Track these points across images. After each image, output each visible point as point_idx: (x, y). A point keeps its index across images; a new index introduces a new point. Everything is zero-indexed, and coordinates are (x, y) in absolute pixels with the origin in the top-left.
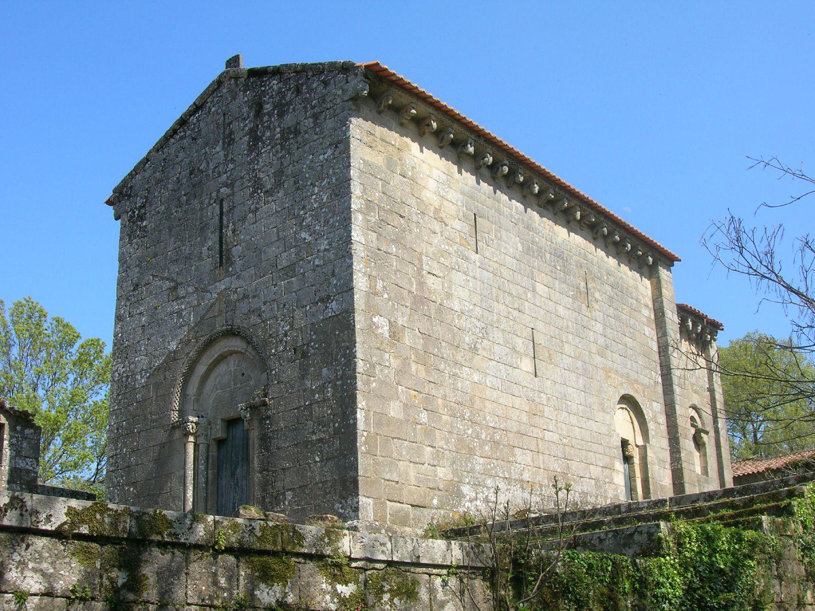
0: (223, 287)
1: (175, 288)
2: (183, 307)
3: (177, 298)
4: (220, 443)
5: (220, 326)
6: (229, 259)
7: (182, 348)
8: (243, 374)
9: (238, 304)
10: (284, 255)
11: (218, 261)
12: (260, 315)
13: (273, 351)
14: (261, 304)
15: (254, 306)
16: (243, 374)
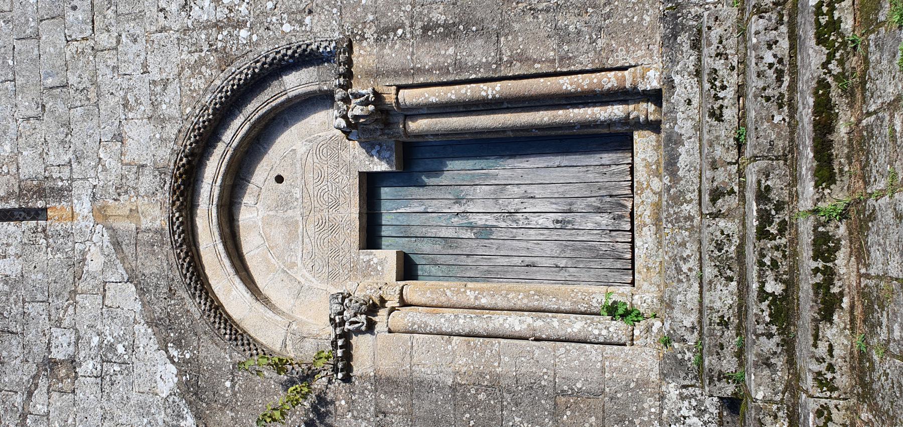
0: (87, 205)
1: (50, 365)
2: (95, 340)
3: (72, 362)
4: (408, 269)
5: (156, 215)
6: (41, 192)
7: (178, 344)
8: (279, 179)
9: (126, 159)
10: (70, 16)
11: (33, 223)
12: (165, 83)
13: (244, 33)
14: (147, 78)
15: (146, 108)
16: (279, 179)
